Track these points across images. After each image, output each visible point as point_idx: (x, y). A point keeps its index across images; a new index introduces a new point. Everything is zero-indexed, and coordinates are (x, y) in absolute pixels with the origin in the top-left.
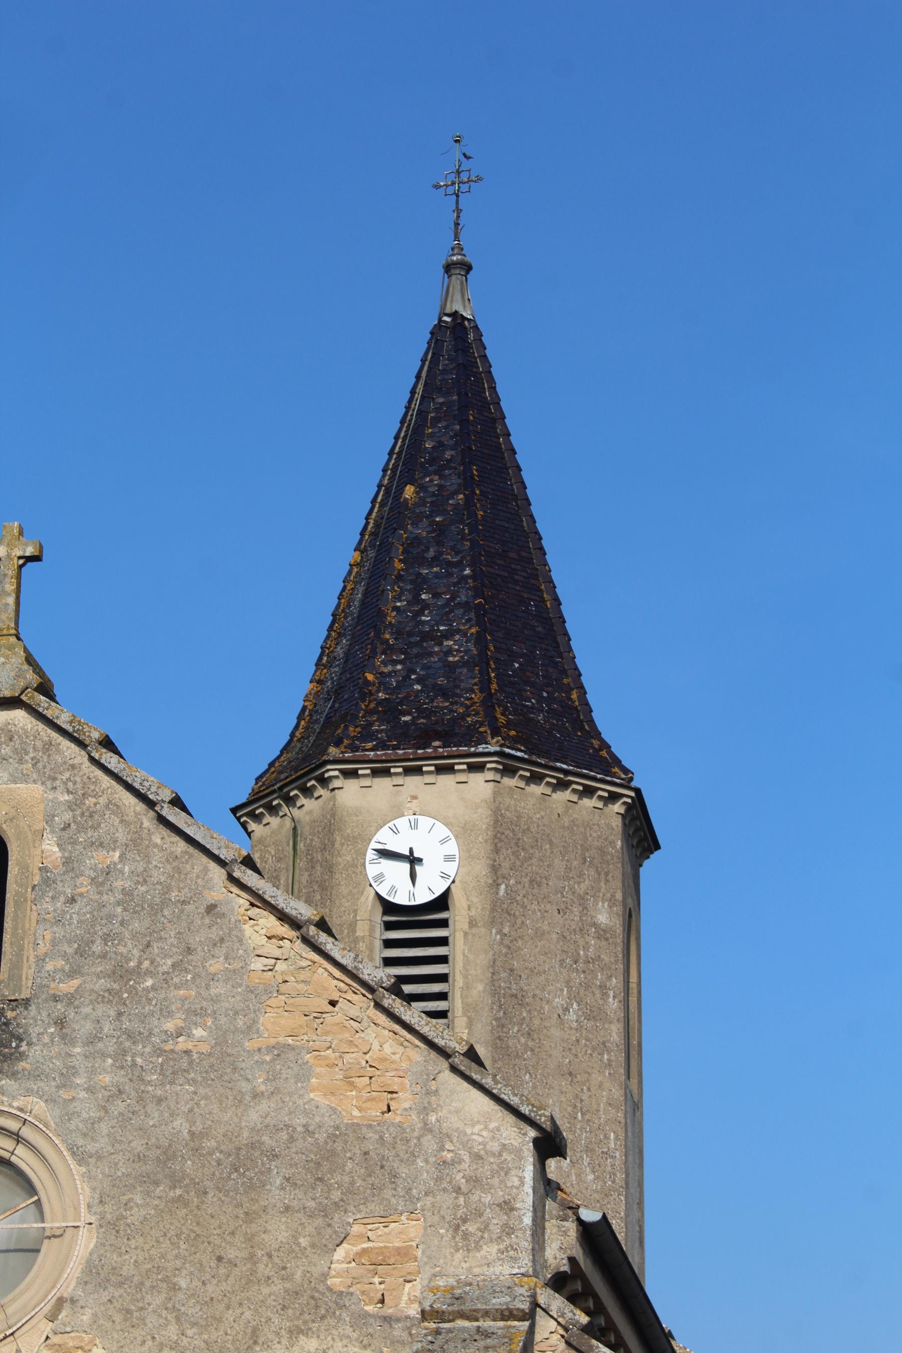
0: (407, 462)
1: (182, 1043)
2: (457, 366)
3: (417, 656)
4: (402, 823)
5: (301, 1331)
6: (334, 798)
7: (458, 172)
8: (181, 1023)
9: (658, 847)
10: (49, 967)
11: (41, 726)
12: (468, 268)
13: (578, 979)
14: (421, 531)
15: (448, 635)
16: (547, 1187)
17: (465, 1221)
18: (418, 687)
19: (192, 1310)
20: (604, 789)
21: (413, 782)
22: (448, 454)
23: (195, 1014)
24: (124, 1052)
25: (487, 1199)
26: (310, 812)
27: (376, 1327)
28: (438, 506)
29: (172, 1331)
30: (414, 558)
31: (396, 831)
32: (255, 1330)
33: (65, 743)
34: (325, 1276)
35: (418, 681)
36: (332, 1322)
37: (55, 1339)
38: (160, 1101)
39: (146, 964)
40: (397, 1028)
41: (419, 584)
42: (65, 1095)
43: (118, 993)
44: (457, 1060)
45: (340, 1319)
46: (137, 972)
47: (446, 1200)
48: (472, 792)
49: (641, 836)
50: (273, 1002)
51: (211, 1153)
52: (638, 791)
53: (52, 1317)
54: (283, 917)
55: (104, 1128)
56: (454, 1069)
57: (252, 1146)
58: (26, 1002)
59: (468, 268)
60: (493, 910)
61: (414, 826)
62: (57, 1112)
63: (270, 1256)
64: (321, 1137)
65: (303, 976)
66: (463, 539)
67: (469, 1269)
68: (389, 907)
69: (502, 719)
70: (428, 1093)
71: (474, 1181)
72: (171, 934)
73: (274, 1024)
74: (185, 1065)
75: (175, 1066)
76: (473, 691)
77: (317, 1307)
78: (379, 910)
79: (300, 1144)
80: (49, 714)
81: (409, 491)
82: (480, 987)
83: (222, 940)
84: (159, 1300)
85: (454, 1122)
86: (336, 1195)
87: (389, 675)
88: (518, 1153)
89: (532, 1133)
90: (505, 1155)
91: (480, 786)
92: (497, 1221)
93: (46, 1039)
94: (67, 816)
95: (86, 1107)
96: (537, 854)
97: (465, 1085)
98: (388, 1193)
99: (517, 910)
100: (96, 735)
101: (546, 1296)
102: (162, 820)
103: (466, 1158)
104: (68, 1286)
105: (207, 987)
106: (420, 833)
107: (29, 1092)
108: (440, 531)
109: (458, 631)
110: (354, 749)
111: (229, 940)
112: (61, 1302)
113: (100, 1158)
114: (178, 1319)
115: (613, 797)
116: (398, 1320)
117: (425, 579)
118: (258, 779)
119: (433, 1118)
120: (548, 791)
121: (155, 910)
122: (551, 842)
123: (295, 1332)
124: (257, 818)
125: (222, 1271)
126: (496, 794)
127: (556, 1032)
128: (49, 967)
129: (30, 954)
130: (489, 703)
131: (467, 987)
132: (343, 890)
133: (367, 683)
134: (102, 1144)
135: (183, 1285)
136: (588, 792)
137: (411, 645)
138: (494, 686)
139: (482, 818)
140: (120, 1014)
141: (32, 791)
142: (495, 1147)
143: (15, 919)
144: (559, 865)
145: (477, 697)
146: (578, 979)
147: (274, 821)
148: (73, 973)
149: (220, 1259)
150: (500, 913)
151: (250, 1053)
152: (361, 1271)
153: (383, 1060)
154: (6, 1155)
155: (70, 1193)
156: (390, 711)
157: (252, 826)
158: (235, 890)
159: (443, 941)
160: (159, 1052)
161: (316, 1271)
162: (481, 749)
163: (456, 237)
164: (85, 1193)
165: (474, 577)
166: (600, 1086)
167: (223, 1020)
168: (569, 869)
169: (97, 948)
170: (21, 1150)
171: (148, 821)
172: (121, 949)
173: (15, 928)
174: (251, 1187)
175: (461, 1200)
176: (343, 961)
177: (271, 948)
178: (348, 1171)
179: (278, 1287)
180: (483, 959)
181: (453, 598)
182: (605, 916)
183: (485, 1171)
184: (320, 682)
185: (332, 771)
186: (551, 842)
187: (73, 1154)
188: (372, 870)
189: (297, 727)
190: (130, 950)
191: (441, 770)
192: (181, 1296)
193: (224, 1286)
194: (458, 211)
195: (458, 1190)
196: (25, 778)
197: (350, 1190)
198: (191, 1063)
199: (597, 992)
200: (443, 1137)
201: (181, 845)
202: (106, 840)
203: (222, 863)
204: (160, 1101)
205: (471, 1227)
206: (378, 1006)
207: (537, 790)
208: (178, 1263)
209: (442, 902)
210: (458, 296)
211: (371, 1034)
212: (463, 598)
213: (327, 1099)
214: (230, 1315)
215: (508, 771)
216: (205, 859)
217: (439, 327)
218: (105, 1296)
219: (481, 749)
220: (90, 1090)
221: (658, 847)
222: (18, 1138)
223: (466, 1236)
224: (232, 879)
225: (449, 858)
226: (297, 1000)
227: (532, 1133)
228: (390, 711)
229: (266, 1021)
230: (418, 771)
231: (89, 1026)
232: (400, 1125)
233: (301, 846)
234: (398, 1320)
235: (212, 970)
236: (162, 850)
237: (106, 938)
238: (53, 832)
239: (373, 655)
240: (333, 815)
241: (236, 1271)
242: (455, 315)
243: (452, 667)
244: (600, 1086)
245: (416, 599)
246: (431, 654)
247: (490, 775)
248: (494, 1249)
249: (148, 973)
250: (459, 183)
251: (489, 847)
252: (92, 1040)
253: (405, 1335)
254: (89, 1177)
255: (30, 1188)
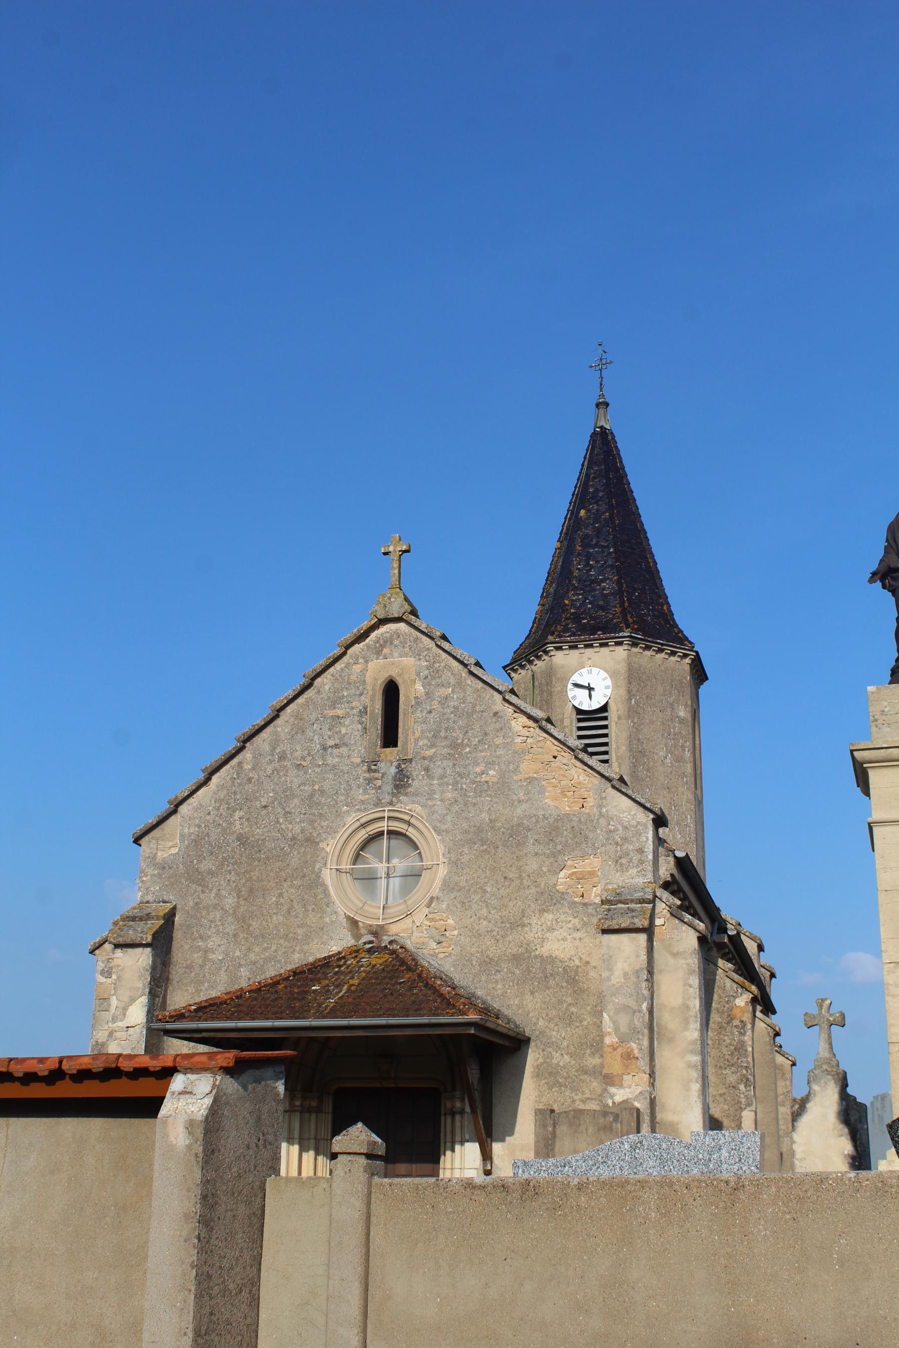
0: (581, 498)
1: (484, 778)
2: (603, 453)
3: (589, 591)
4: (584, 671)
5: (544, 911)
6: (551, 660)
7: (601, 360)
8: (483, 768)
9: (707, 679)
10: (420, 743)
11: (413, 630)
12: (607, 405)
13: (671, 742)
14: (589, 531)
15: (603, 581)
16: (659, 841)
17: (621, 858)
18: (590, 606)
19: (494, 902)
21: (589, 651)
22: (601, 494)
23: (490, 764)
24: (457, 783)
25: (631, 847)
26: (540, 667)
27: (580, 908)
28: (596, 520)
29: (484, 912)
30: (586, 545)
31: (581, 675)
32: (523, 910)
33: (424, 638)
34: (555, 885)
35: (590, 603)
36: (560, 906)
37: (430, 916)
38: (475, 805)
39: (466, 741)
40: (586, 768)
41: (589, 557)
42: (430, 803)
43: (453, 755)
44: (615, 783)
45: (563, 904)
46: (462, 745)
47: (612, 848)
48: (618, 655)
49: (699, 674)
50: (526, 757)
51: (499, 829)
52: (697, 652)
53: (428, 906)
54: (530, 717)
55: (449, 818)
56: (613, 787)
57: (519, 825)
58: (411, 761)
59: (607, 405)
60: (629, 711)
61: (590, 672)
62: (427, 811)
63: (529, 876)
64: (551, 820)
65: (540, 744)
66: (609, 534)
67: (624, 881)
68: (579, 711)
69: (631, 620)
70: (601, 799)
71: (625, 839)
72: (477, 727)
73: (527, 767)
74: (486, 788)
75: (482, 788)
76: (616, 607)
77: (552, 899)
78: (575, 713)
79: (541, 824)
80: (416, 624)
81: (583, 513)
82: (624, 748)
83: (501, 729)
84: (478, 897)
85: (614, 812)
86: (559, 847)
87: (576, 600)
88: (645, 825)
89: (652, 816)
90: (639, 827)
91: (621, 652)
92: (636, 858)
93: (420, 777)
94: (427, 672)
95: (440, 809)
96: (649, 684)
97: (619, 794)
98: (584, 846)
99: (641, 711)
100: (438, 634)
101: (660, 892)
102: (471, 673)
103: (620, 828)
104: (435, 890)
105: (495, 751)
106: (593, 676)
107: (413, 802)
108: (598, 531)
109: (608, 579)
110: (560, 636)
111: (504, 728)
112: (432, 899)
113: (447, 832)
114: (487, 906)
116: (590, 905)
117: (591, 554)
118: (515, 653)
119: (604, 810)
120: (654, 654)
121: (469, 715)
122: (656, 678)
123: (542, 911)
124: (515, 671)
125: (507, 883)
126: (629, 656)
127: (661, 769)
128: (420, 743)
129: (412, 738)
130: (624, 612)
131: (618, 748)
132: (557, 704)
133: (566, 605)
134: (449, 825)
135: (489, 890)
136: (673, 653)
137: (586, 586)
138: (626, 604)
139: (622, 667)
140: (454, 765)
141: (409, 661)
142: (634, 823)
143: (404, 721)
144: (660, 689)
145: (618, 610)
146: (671, 742)
147: (523, 672)
148: (432, 746)
149: (505, 878)
150: (633, 713)
151: (516, 782)
152: (572, 882)
153: (580, 783)
154: (404, 831)
155: (435, 848)
156: (577, 618)
157: (513, 675)
158: (507, 705)
159: (606, 727)
160: (474, 782)
161: (551, 883)
162: (621, 634)
163: (601, 390)
164: (441, 849)
165: (615, 552)
166: (683, 793)
167: (503, 767)
168: (665, 690)
169: (443, 734)
170: (410, 829)
171: (464, 673)
172: (454, 734)
173: (404, 726)
174: (519, 844)
175: (619, 848)
176: (559, 737)
177: (525, 732)
178: (565, 836)
179: (533, 890)
180: (625, 735)
181: (605, 563)
182: (683, 712)
183: (629, 834)
184: (542, 605)
185: (550, 647)
186: (656, 678)
187: (435, 830)
188: (570, 694)
189: (532, 627)
190: (458, 734)
191: (602, 645)
192: (488, 895)
193: (508, 890)
194: (602, 378)
195: (617, 844)
196: (406, 655)
197: (566, 845)
198: (489, 787)
199: (680, 750)
200: (609, 819)
201: (481, 684)
202: (445, 683)
203: (500, 692)
204: (475, 805)
205: (624, 861)
206: (576, 758)
207: (648, 653)
208: (486, 880)
209: (604, 708)
210: (603, 418)
211: (573, 771)
212: (610, 563)
213: (553, 803)
214: (511, 904)
215: (634, 645)
216: (492, 691)
217: (594, 434)
218: (453, 896)
219: (621, 634)
220: (441, 800)
221: (707, 679)
222: (409, 823)
223: (621, 865)
224: (505, 700)
225: (607, 687)
226: (538, 757)
227: (652, 816)
228: (577, 618)
229: (524, 766)
230: (591, 646)
231: (440, 771)
232: (588, 814)
233: (536, 683)
234: (590, 905)
235: (497, 743)
236: (471, 687)
237: (447, 729)
238: (420, 680)
239: (568, 592)
240: (551, 669)
241: (514, 883)
242: (601, 427)
243: (606, 596)
244: (683, 793)
245: (588, 564)
246: (596, 590)
247: (626, 647)
248: (635, 871)
249: (467, 745)
250: (602, 365)
251: (626, 681)
252: (442, 777)
253: (594, 912)
254: (443, 841)
255: (416, 847)
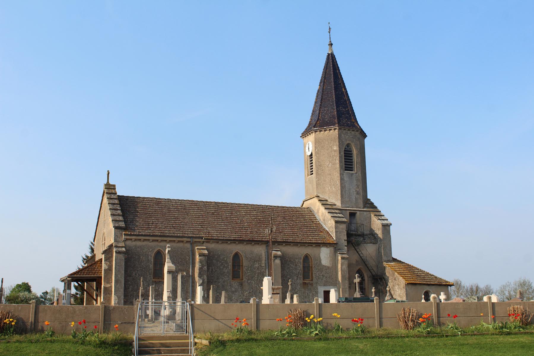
12: (331, 44)
20: (333, 129)
106: (310, 144)
115: (335, 129)
136: (330, 130)
144: (327, 143)
207: (322, 132)
215: (316, 132)
